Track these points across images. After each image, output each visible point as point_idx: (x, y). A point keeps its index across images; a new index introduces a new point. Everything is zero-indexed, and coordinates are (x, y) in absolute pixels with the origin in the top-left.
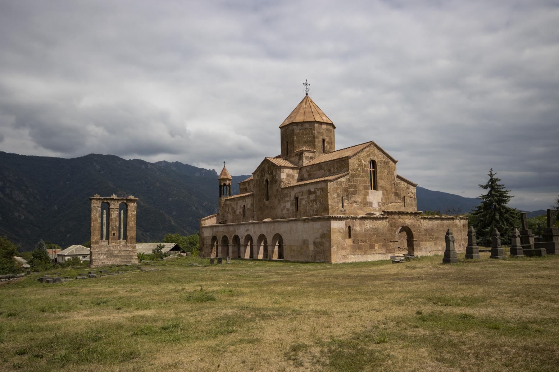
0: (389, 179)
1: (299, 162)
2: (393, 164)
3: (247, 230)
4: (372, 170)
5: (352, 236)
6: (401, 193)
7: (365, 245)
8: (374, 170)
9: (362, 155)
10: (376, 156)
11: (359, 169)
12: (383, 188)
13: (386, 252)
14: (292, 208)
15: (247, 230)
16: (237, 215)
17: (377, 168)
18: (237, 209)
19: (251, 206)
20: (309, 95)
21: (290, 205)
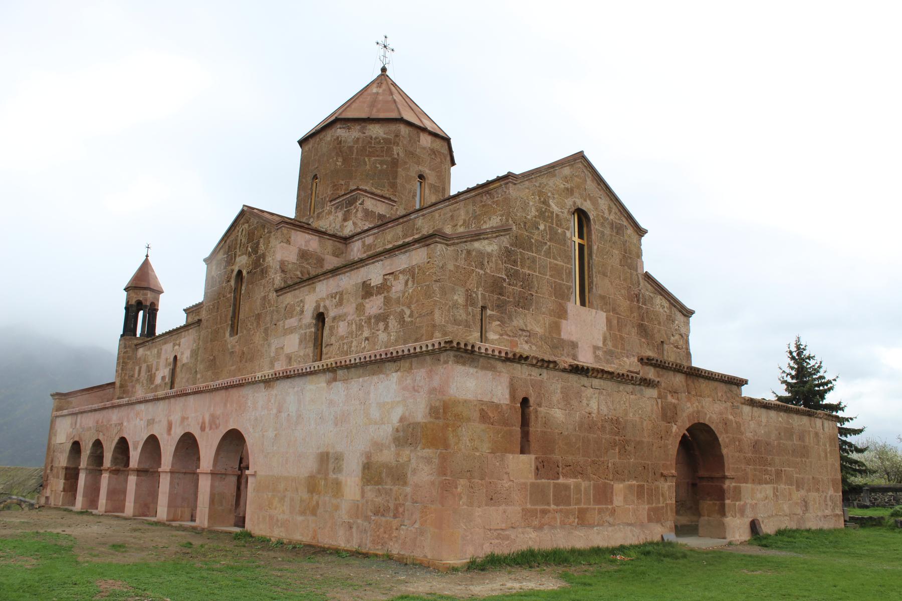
0: (625, 280)
1: (342, 227)
2: (635, 237)
3: (151, 422)
4: (577, 239)
5: (534, 445)
6: (656, 331)
7: (578, 487)
8: (581, 241)
9: (551, 183)
10: (590, 200)
11: (542, 227)
12: (606, 304)
13: (650, 520)
14: (302, 354)
15: (151, 422)
16: (157, 386)
17: (593, 237)
18: (157, 370)
19: (192, 356)
20: (388, 73)
21: (297, 341)
